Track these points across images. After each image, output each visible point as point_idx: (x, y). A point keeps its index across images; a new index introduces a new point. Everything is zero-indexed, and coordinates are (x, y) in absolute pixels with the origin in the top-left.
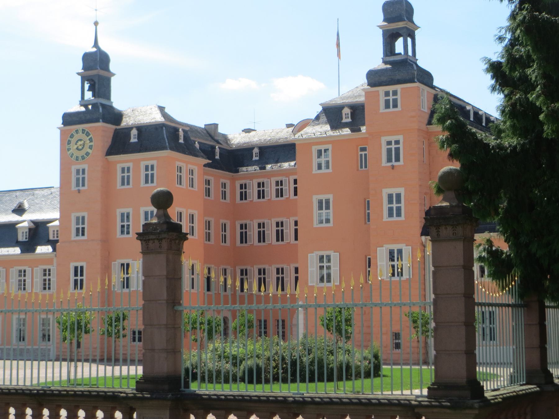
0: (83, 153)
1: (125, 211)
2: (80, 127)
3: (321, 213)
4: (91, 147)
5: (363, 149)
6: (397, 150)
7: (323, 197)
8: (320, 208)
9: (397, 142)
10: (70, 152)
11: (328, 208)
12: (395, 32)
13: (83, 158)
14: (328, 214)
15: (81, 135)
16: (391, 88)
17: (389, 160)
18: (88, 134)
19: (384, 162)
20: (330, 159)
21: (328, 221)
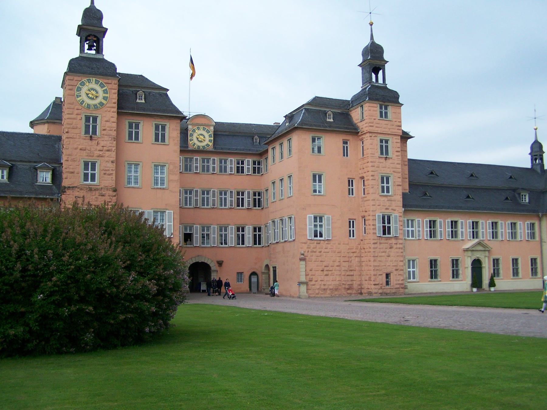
0: (97, 102)
3: (315, 185)
6: (387, 147)
8: (315, 181)
10: (79, 99)
11: (320, 181)
12: (377, 66)
17: (382, 153)
18: (102, 86)
21: (319, 192)
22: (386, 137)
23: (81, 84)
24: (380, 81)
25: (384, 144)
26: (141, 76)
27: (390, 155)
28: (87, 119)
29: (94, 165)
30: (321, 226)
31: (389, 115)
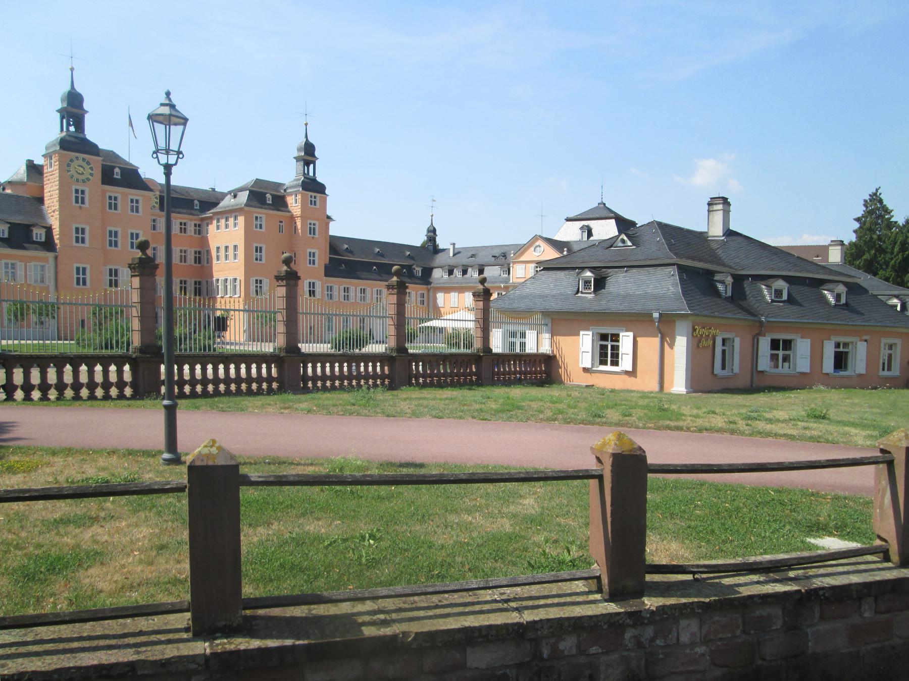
0: (83, 177)
1: (113, 229)
2: (81, 156)
4: (91, 175)
5: (281, 222)
6: (314, 229)
7: (259, 245)
8: (257, 251)
9: (314, 224)
10: (69, 173)
13: (84, 181)
14: (261, 256)
15: (80, 162)
16: (314, 194)
17: (310, 233)
18: (88, 163)
19: (309, 235)
20: (255, 222)
22: (314, 222)
23: (70, 161)
24: (311, 174)
25: (312, 226)
26: (112, 151)
27: (317, 235)
28: (77, 191)
29: (83, 230)
30: (261, 287)
31: (318, 203)
